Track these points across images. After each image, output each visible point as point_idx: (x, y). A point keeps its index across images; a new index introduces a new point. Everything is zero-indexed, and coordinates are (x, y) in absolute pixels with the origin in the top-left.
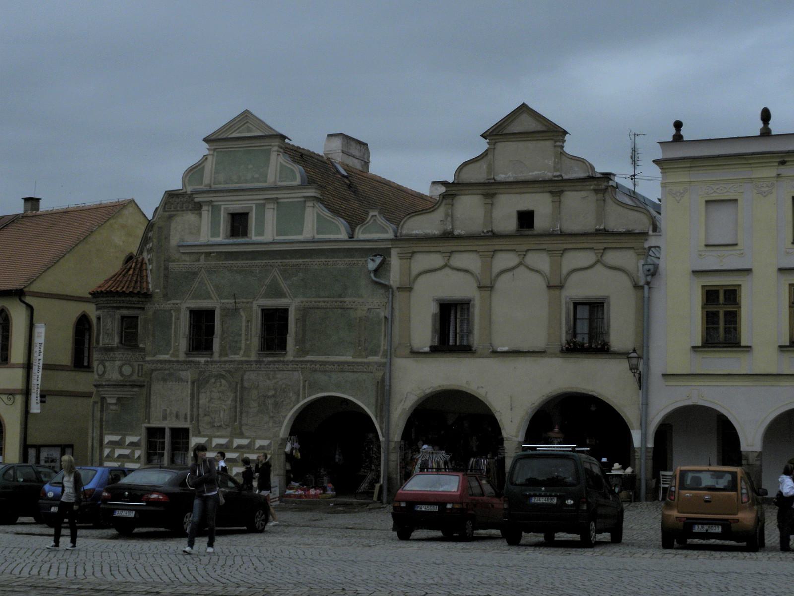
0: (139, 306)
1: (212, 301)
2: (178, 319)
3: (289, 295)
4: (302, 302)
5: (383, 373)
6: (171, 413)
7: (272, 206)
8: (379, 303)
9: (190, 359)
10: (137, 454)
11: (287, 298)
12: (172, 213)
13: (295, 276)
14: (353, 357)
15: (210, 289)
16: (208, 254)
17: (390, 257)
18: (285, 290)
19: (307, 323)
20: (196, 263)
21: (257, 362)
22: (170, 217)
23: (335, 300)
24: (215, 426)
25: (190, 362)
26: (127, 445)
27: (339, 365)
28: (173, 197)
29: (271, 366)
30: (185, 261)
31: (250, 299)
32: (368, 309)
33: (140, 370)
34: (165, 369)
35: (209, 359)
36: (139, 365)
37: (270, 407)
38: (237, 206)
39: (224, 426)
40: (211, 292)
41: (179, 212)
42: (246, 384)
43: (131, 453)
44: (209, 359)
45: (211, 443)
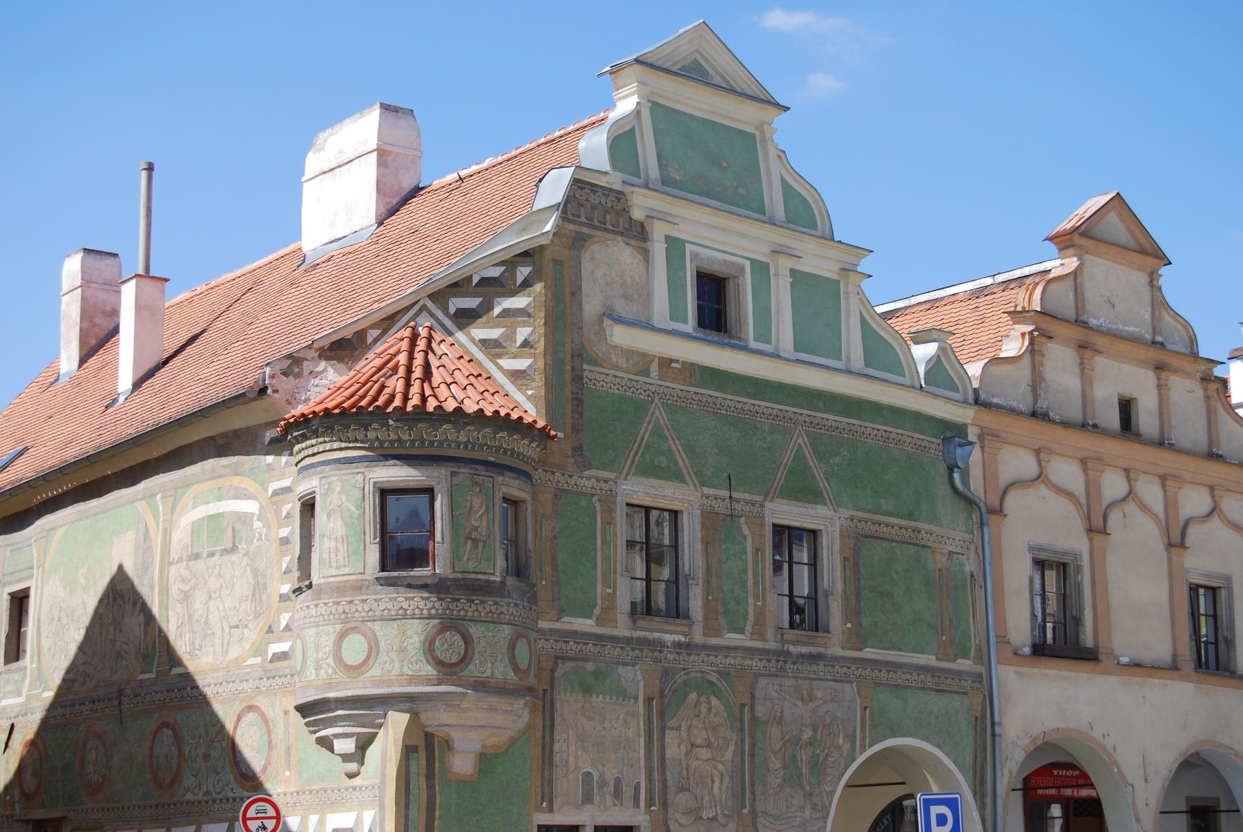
2: (609, 522)
11: (826, 505)
12: (584, 230)
13: (836, 456)
14: (938, 659)
15: (678, 458)
16: (666, 363)
19: (861, 569)
22: (579, 241)
24: (701, 818)
27: (918, 675)
30: (617, 368)
32: (951, 553)
34: (586, 660)
39: (722, 819)
40: (680, 462)
41: (598, 233)
42: (761, 710)
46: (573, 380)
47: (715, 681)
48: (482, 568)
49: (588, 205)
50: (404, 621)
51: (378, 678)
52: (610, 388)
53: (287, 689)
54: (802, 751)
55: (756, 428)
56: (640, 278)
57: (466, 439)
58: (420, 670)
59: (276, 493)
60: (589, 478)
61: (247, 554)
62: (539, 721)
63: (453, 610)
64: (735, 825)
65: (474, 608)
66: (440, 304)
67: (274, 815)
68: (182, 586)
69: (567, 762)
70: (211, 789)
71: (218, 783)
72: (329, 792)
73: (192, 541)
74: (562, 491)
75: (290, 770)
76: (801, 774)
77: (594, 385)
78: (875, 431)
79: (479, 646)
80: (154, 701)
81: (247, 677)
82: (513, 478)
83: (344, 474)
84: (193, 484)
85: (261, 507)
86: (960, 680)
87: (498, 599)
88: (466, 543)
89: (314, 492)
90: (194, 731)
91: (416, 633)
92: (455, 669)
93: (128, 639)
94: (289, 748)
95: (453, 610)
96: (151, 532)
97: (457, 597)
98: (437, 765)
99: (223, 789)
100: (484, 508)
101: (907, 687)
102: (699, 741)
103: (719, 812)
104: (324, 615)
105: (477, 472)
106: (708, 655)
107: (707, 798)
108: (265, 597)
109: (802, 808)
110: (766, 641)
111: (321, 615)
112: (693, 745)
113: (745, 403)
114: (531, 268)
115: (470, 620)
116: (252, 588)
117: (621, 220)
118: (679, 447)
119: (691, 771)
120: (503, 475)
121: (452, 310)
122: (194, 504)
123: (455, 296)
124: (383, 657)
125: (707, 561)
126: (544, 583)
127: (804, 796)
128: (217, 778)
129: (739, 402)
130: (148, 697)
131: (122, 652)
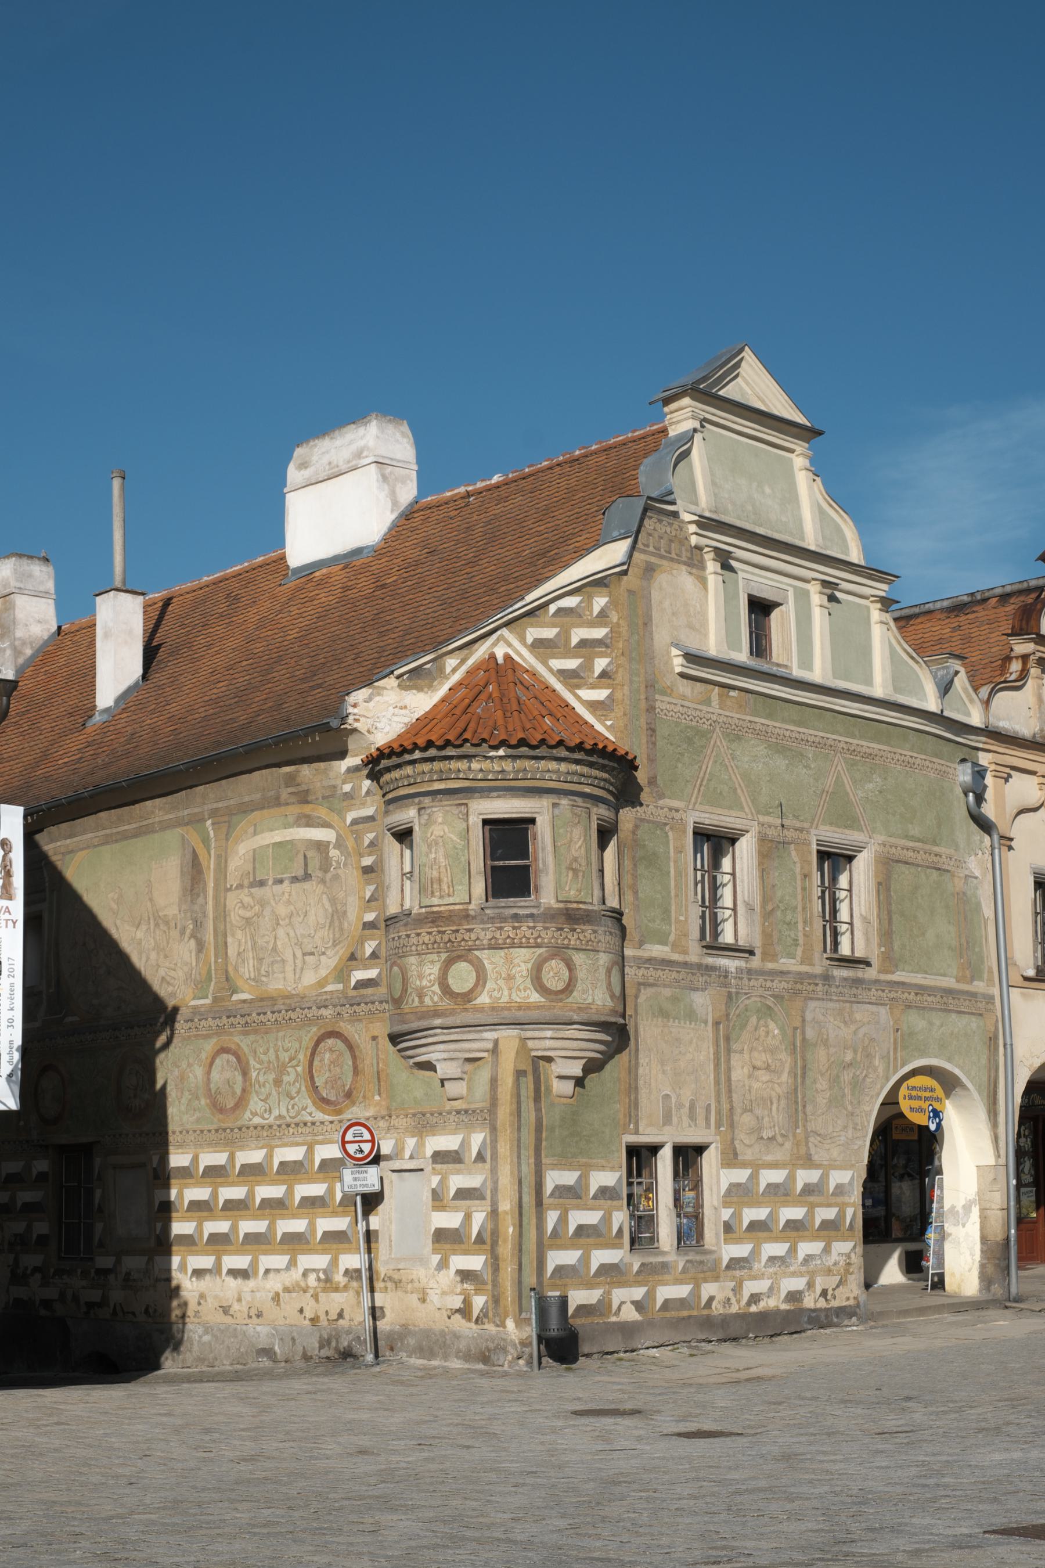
2: (679, 851)
6: (680, 1106)
9: (710, 960)
12: (653, 559)
14: (958, 981)
19: (892, 894)
20: (704, 708)
21: (827, 978)
23: (927, 847)
24: (762, 1138)
26: (595, 1197)
34: (665, 986)
37: (846, 1090)
38: (765, 585)
39: (780, 1139)
40: (739, 791)
41: (665, 563)
43: (603, 1218)
47: (772, 1005)
49: (656, 535)
50: (511, 950)
51: (487, 1005)
53: (375, 1016)
55: (802, 755)
57: (566, 771)
58: (528, 997)
59: (355, 822)
61: (323, 881)
63: (557, 939)
65: (576, 936)
66: (518, 633)
67: (369, 1138)
68: (241, 912)
69: (650, 1085)
70: (284, 1112)
71: (293, 1108)
72: (428, 1115)
73: (254, 868)
75: (379, 1095)
76: (844, 1096)
77: (666, 715)
79: (581, 974)
80: (210, 1026)
81: (326, 1003)
83: (446, 806)
84: (253, 811)
85: (339, 836)
87: (596, 928)
88: (567, 875)
89: (412, 822)
90: (262, 1056)
91: (523, 959)
92: (560, 996)
93: (176, 964)
94: (378, 1073)
95: (557, 939)
96: (201, 858)
97: (560, 926)
98: (543, 1089)
99: (298, 1114)
100: (582, 839)
101: (932, 1009)
102: (759, 1064)
104: (427, 945)
106: (766, 980)
107: (766, 1119)
108: (346, 924)
109: (845, 1127)
111: (424, 943)
112: (754, 1067)
114: (606, 599)
115: (573, 949)
116: (330, 916)
117: (683, 549)
118: (738, 776)
120: (597, 806)
121: (529, 640)
122: (255, 831)
123: (532, 626)
124: (489, 985)
128: (292, 1102)
129: (787, 730)
130: (203, 1023)
131: (168, 978)
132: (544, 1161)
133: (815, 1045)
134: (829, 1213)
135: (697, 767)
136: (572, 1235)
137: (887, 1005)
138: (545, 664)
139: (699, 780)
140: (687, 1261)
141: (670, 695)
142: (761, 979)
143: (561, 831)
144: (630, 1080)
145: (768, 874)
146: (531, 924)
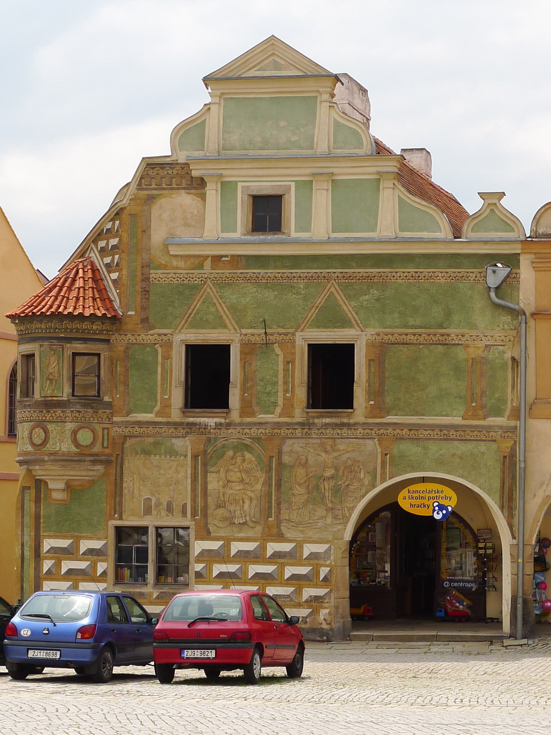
0: (102, 337)
1: (226, 331)
2: (167, 357)
3: (357, 324)
4: (379, 335)
5: (510, 444)
6: (158, 504)
7: (325, 185)
8: (503, 338)
9: (191, 420)
10: (101, 567)
12: (155, 192)
13: (366, 295)
15: (223, 314)
16: (216, 259)
17: (519, 267)
18: (350, 315)
22: (151, 199)
23: (432, 331)
24: (234, 523)
25: (188, 424)
26: (84, 554)
28: (153, 168)
29: (328, 432)
30: (177, 268)
31: (292, 327)
33: (106, 437)
34: (148, 436)
35: (223, 421)
36: (103, 429)
37: (327, 494)
40: (225, 317)
42: (286, 459)
44: (223, 421)
45: (229, 550)
46: (143, 280)
48: (56, 393)
52: (171, 281)
54: (325, 483)
56: (198, 212)
58: (27, 449)
60: (151, 335)
62: (113, 471)
63: (39, 417)
64: (262, 526)
65: (50, 415)
69: (133, 493)
74: (133, 344)
76: (324, 497)
77: (159, 281)
78: (405, 275)
79: (51, 436)
82: (79, 343)
86: (488, 432)
87: (65, 410)
88: (47, 381)
92: (40, 447)
95: (39, 417)
97: (41, 410)
98: (42, 496)
100: (56, 362)
101: (429, 439)
102: (234, 479)
103: (248, 520)
105: (52, 344)
110: (293, 417)
113: (283, 273)
118: (225, 309)
119: (227, 496)
120: (71, 343)
125: (245, 372)
126: (118, 396)
127: (326, 510)
132: (42, 534)
133: (292, 467)
134: (303, 570)
135: (186, 307)
136: (64, 574)
137: (376, 438)
138: (102, 260)
139: (187, 315)
140: (161, 592)
141: (165, 269)
142: (239, 428)
143: (44, 359)
144: (115, 490)
145: (251, 364)
146: (29, 410)
